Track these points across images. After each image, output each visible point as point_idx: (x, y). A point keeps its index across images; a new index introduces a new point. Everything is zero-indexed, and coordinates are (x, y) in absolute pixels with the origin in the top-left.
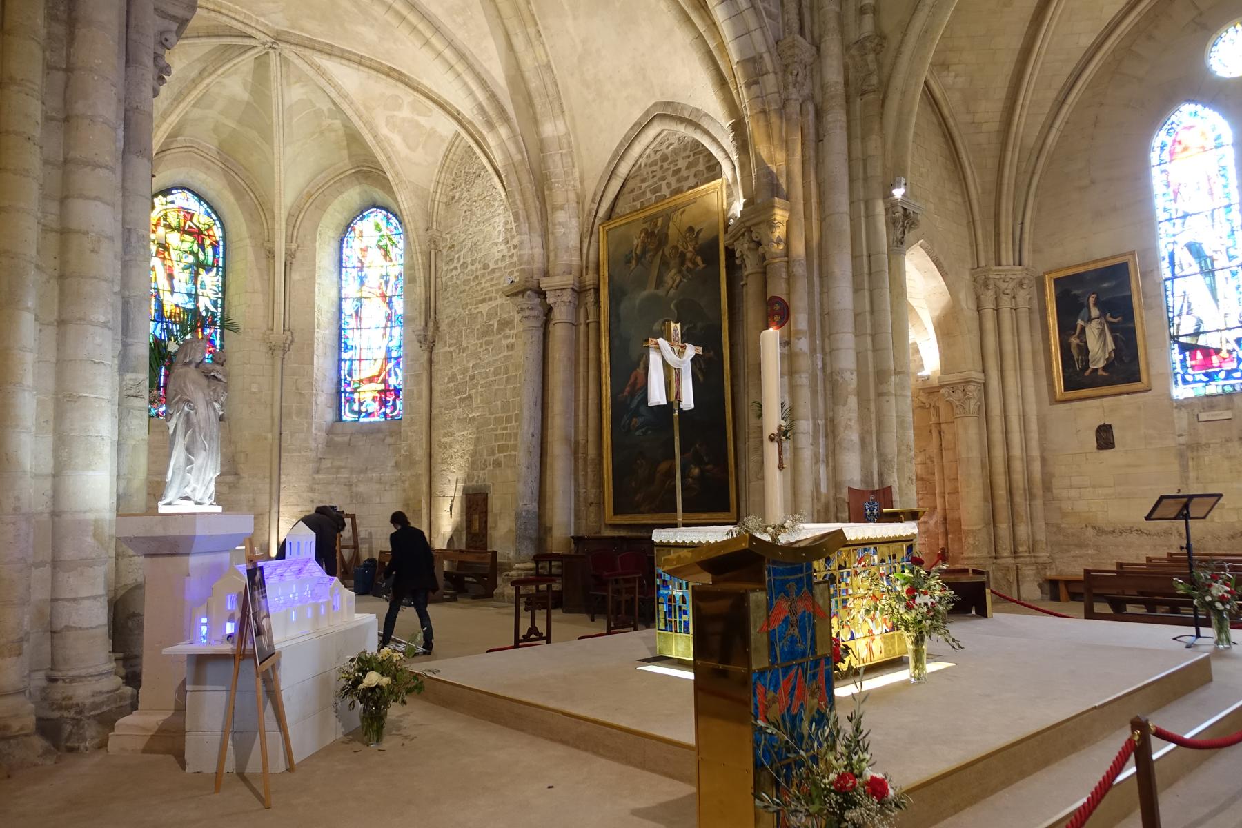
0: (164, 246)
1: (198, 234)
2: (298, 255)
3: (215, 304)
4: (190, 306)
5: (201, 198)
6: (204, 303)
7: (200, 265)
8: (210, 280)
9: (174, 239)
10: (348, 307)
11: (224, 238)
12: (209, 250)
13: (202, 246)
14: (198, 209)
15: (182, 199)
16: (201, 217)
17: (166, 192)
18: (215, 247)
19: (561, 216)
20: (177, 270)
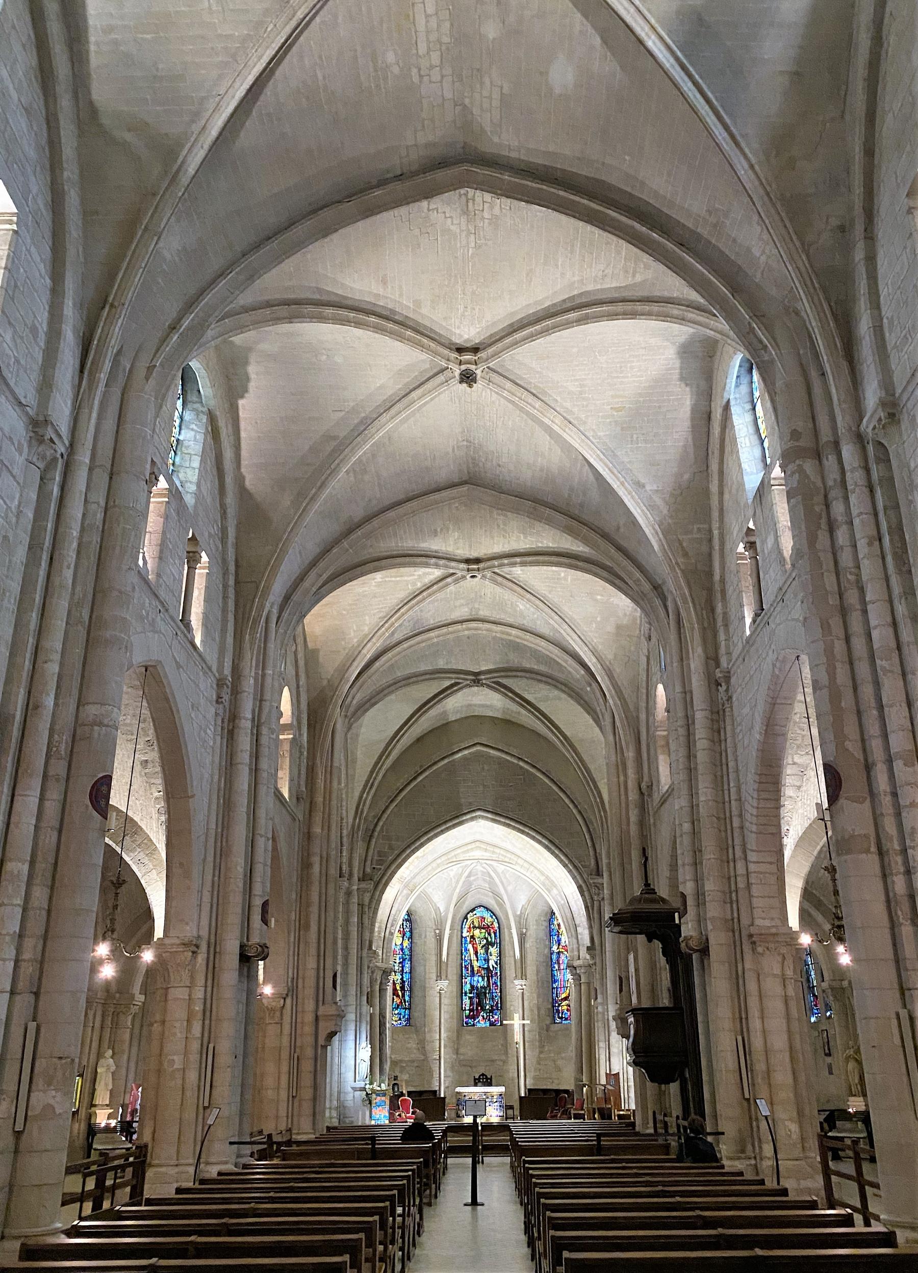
0: (472, 937)
1: (487, 928)
2: (528, 934)
3: (496, 963)
4: (486, 966)
5: (487, 909)
6: (492, 963)
7: (489, 944)
8: (493, 950)
9: (477, 932)
10: (554, 957)
11: (499, 928)
12: (493, 935)
13: (489, 934)
14: (487, 915)
15: (480, 912)
16: (489, 919)
17: (473, 910)
18: (495, 933)
19: (579, 930)
20: (479, 948)
